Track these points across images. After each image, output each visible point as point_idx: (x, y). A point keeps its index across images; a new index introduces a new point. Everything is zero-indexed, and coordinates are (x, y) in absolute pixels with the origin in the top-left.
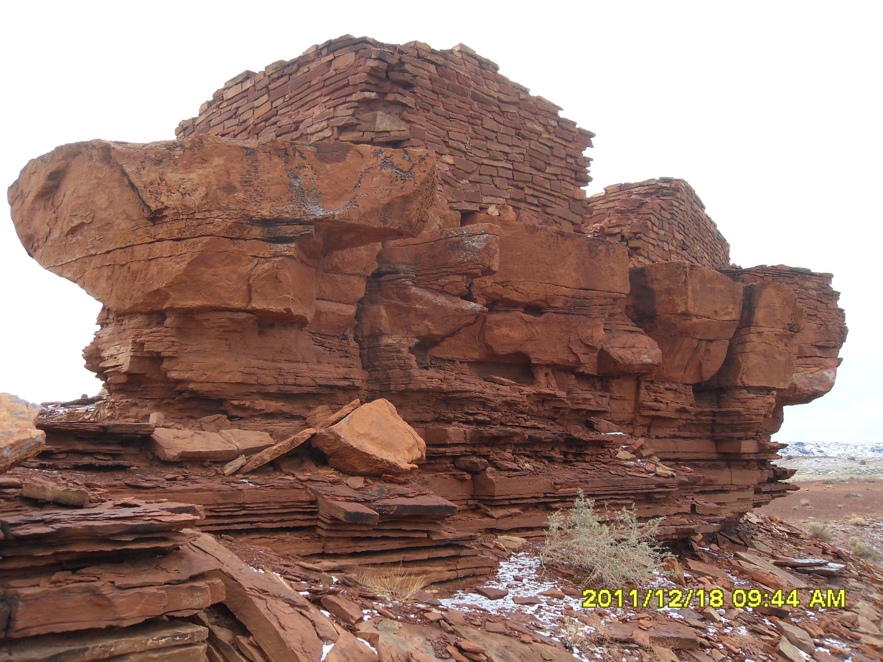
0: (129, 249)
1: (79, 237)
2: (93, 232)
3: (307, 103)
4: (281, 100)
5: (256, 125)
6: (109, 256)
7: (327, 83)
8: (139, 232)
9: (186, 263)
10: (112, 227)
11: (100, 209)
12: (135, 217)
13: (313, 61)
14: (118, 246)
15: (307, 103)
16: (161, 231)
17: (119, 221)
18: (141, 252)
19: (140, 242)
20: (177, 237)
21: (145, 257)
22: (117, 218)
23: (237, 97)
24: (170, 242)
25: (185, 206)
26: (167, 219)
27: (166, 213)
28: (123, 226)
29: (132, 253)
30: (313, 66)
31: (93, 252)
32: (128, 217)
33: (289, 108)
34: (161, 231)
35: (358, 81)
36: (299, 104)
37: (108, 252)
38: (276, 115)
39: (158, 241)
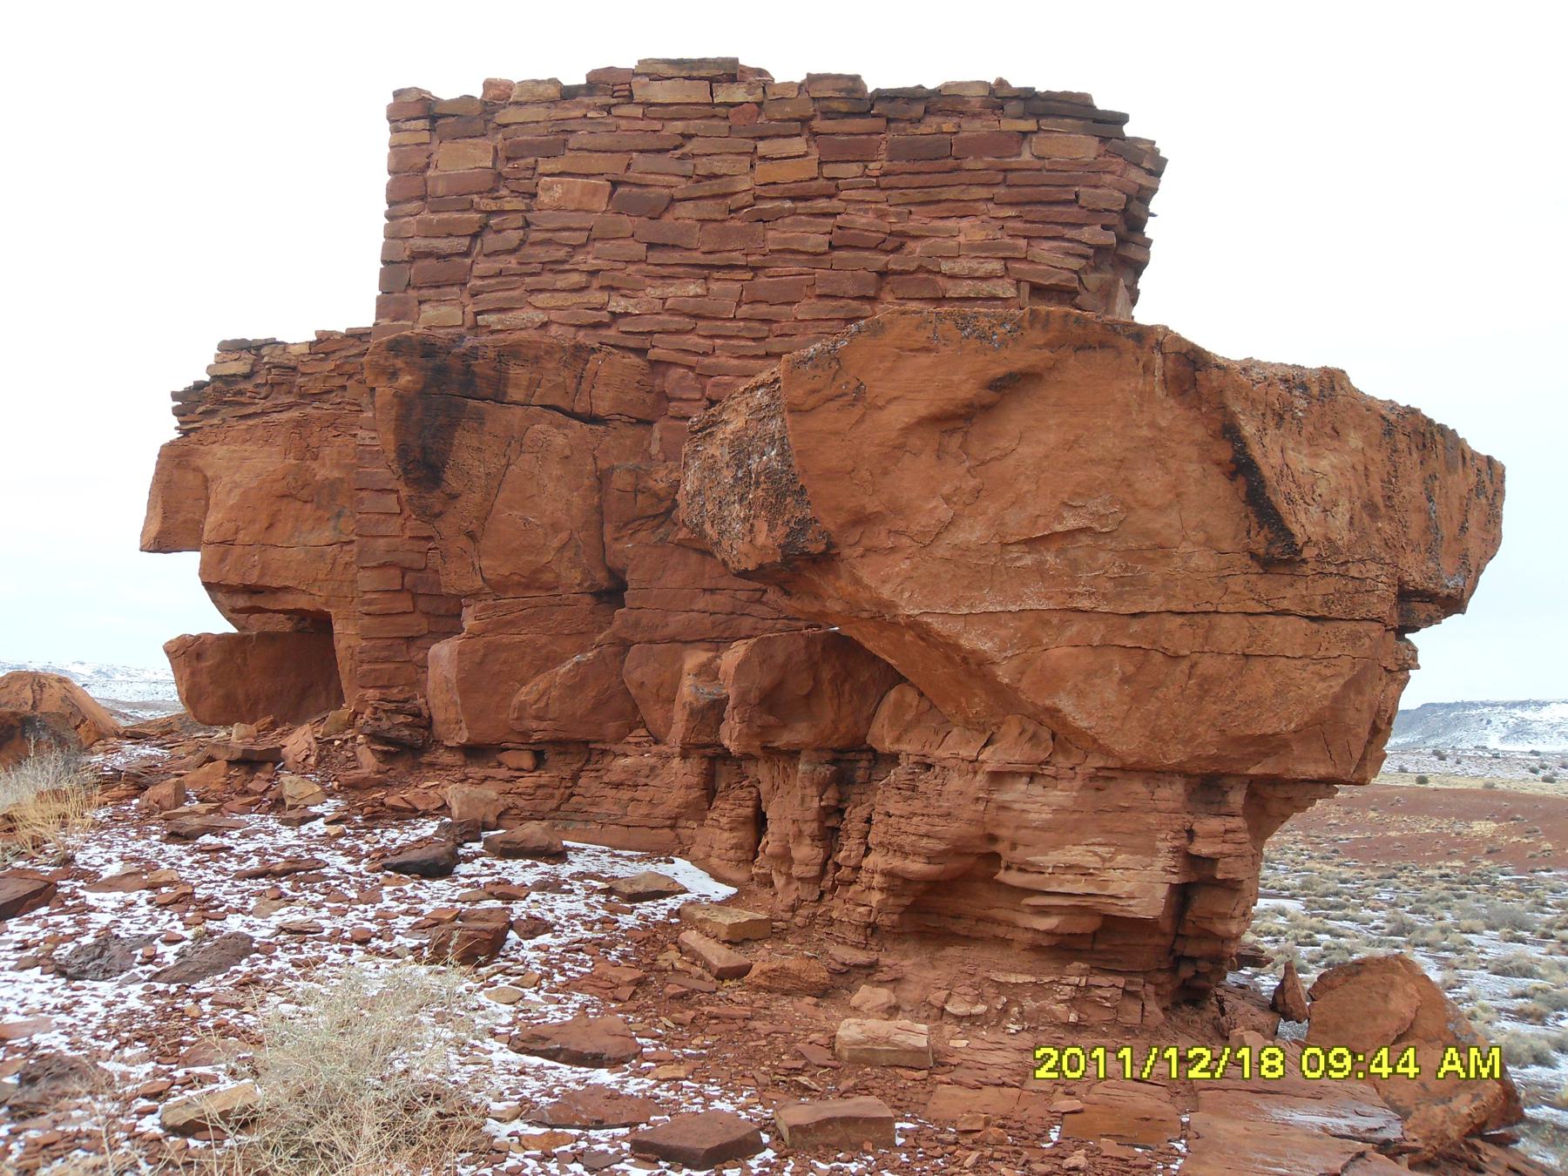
0: (1205, 621)
1: (1050, 558)
2: (1103, 557)
3: (939, 202)
4: (855, 169)
6: (1135, 626)
7: (1011, 177)
8: (1237, 584)
9: (1342, 681)
10: (1168, 556)
11: (1145, 505)
12: (1225, 546)
13: (975, 116)
14: (1174, 607)
15: (939, 202)
16: (1289, 594)
17: (1186, 547)
18: (1230, 632)
19: (1231, 608)
21: (1238, 647)
22: (1184, 539)
23: (688, 109)
24: (1304, 623)
25: (1329, 540)
26: (1307, 569)
27: (1306, 554)
28: (1196, 561)
29: (1211, 628)
30: (973, 128)
31: (1085, 604)
32: (1209, 542)
33: (882, 195)
34: (1290, 592)
35: (1103, 205)
36: (918, 195)
37: (1143, 614)
38: (830, 197)
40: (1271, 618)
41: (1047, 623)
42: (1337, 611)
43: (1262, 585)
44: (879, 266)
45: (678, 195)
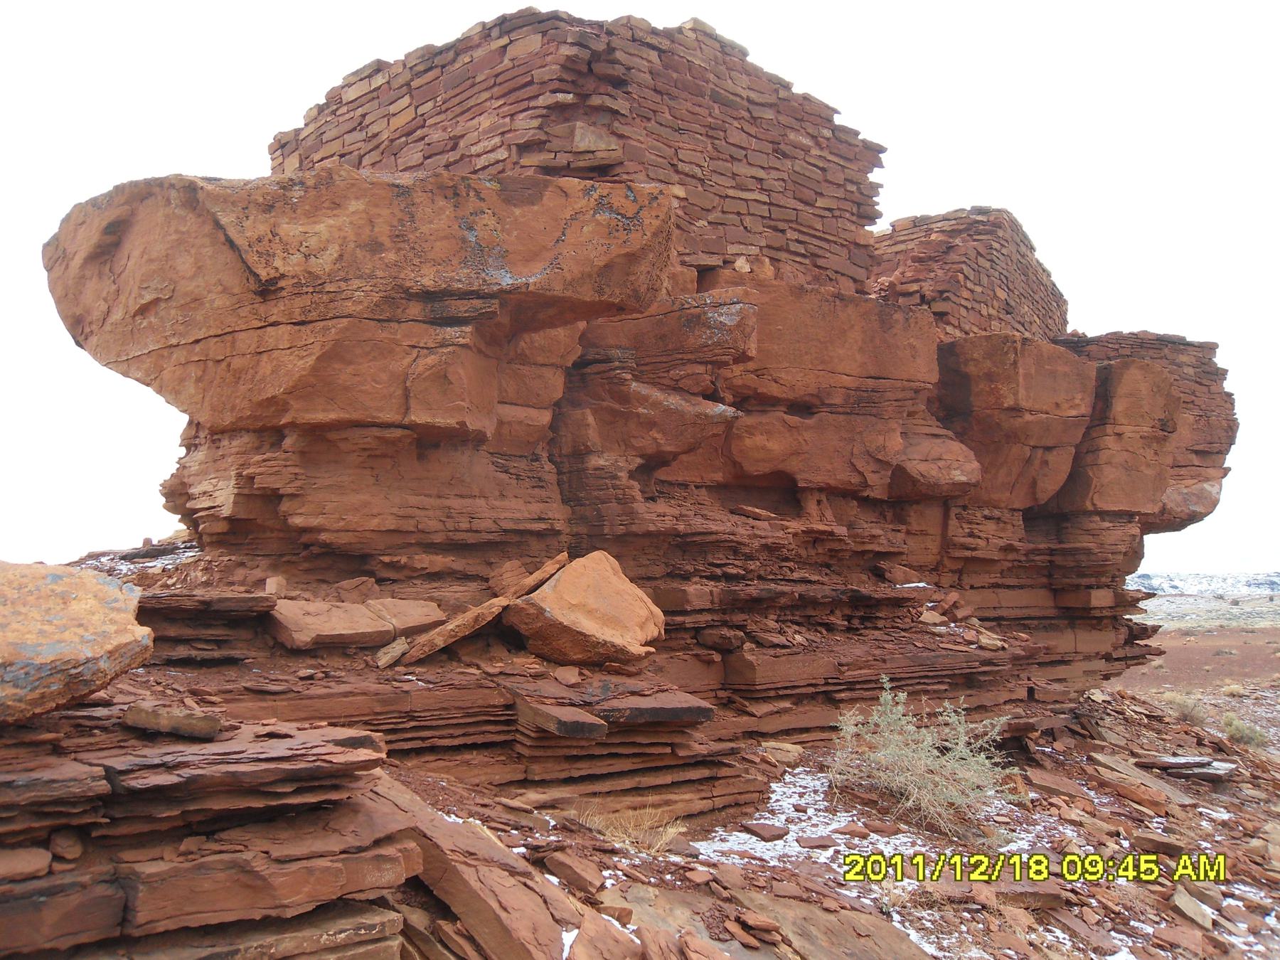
0: (228, 338)
1: (152, 319)
2: (173, 312)
3: (469, 109)
4: (430, 104)
5: (392, 141)
6: (197, 348)
8: (244, 312)
10: (202, 304)
12: (236, 291)
15: (469, 109)
16: (276, 310)
17: (211, 296)
18: (247, 341)
19: (244, 327)
20: (299, 319)
21: (252, 349)
22: (209, 292)
23: (363, 100)
24: (289, 327)
25: (310, 273)
26: (284, 293)
27: (282, 283)
28: (217, 303)
29: (234, 342)
31: (174, 341)
32: (225, 290)
33: (443, 117)
36: (458, 110)
37: (197, 341)
38: (423, 126)
39: (272, 325)
40: (269, 329)
41: (163, 356)
42: (313, 315)
43: (262, 309)
44: (444, 162)
45: (362, 152)
